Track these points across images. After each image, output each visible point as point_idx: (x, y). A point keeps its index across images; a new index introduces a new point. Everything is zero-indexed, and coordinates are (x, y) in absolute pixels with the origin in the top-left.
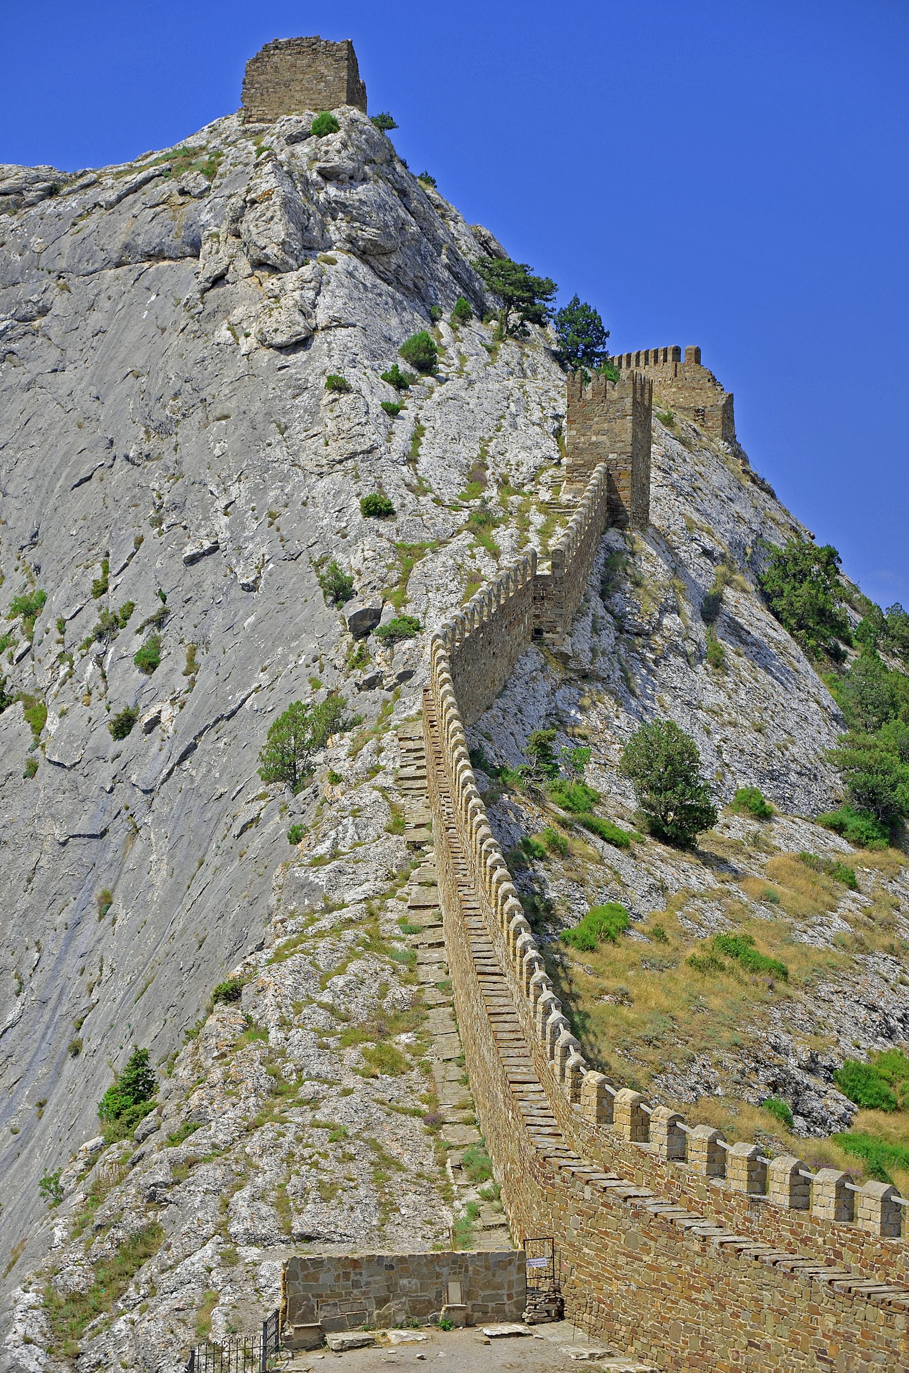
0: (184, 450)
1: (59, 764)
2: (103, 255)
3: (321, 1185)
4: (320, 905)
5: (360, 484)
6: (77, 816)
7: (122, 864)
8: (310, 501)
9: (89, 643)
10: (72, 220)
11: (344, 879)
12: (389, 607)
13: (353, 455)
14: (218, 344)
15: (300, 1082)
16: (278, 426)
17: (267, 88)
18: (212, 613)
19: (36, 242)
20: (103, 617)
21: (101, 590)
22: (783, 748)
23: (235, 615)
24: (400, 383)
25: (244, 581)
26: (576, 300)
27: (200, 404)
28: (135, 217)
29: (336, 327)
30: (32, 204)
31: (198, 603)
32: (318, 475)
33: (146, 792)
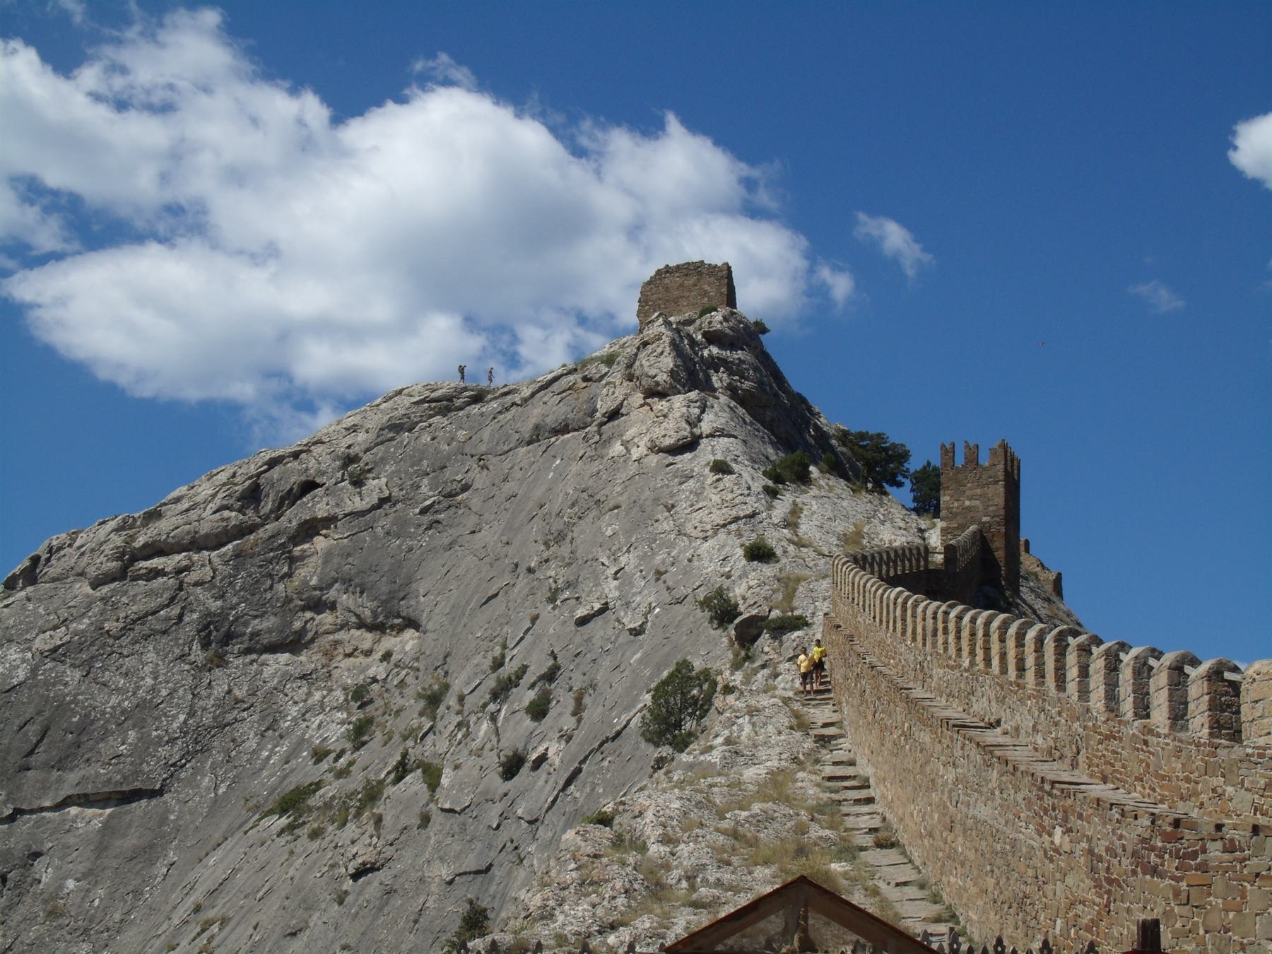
1: (451, 811)
2: (517, 436)
5: (743, 539)
6: (464, 855)
7: (504, 895)
8: (695, 558)
9: (485, 705)
10: (492, 416)
13: (737, 519)
14: (612, 458)
16: (666, 506)
17: (659, 305)
18: (600, 661)
19: (462, 435)
21: (498, 664)
23: (623, 655)
24: (778, 479)
25: (632, 626)
26: (929, 464)
27: (594, 506)
28: (545, 403)
29: (719, 436)
30: (461, 409)
31: (587, 656)
32: (703, 539)
33: (530, 822)
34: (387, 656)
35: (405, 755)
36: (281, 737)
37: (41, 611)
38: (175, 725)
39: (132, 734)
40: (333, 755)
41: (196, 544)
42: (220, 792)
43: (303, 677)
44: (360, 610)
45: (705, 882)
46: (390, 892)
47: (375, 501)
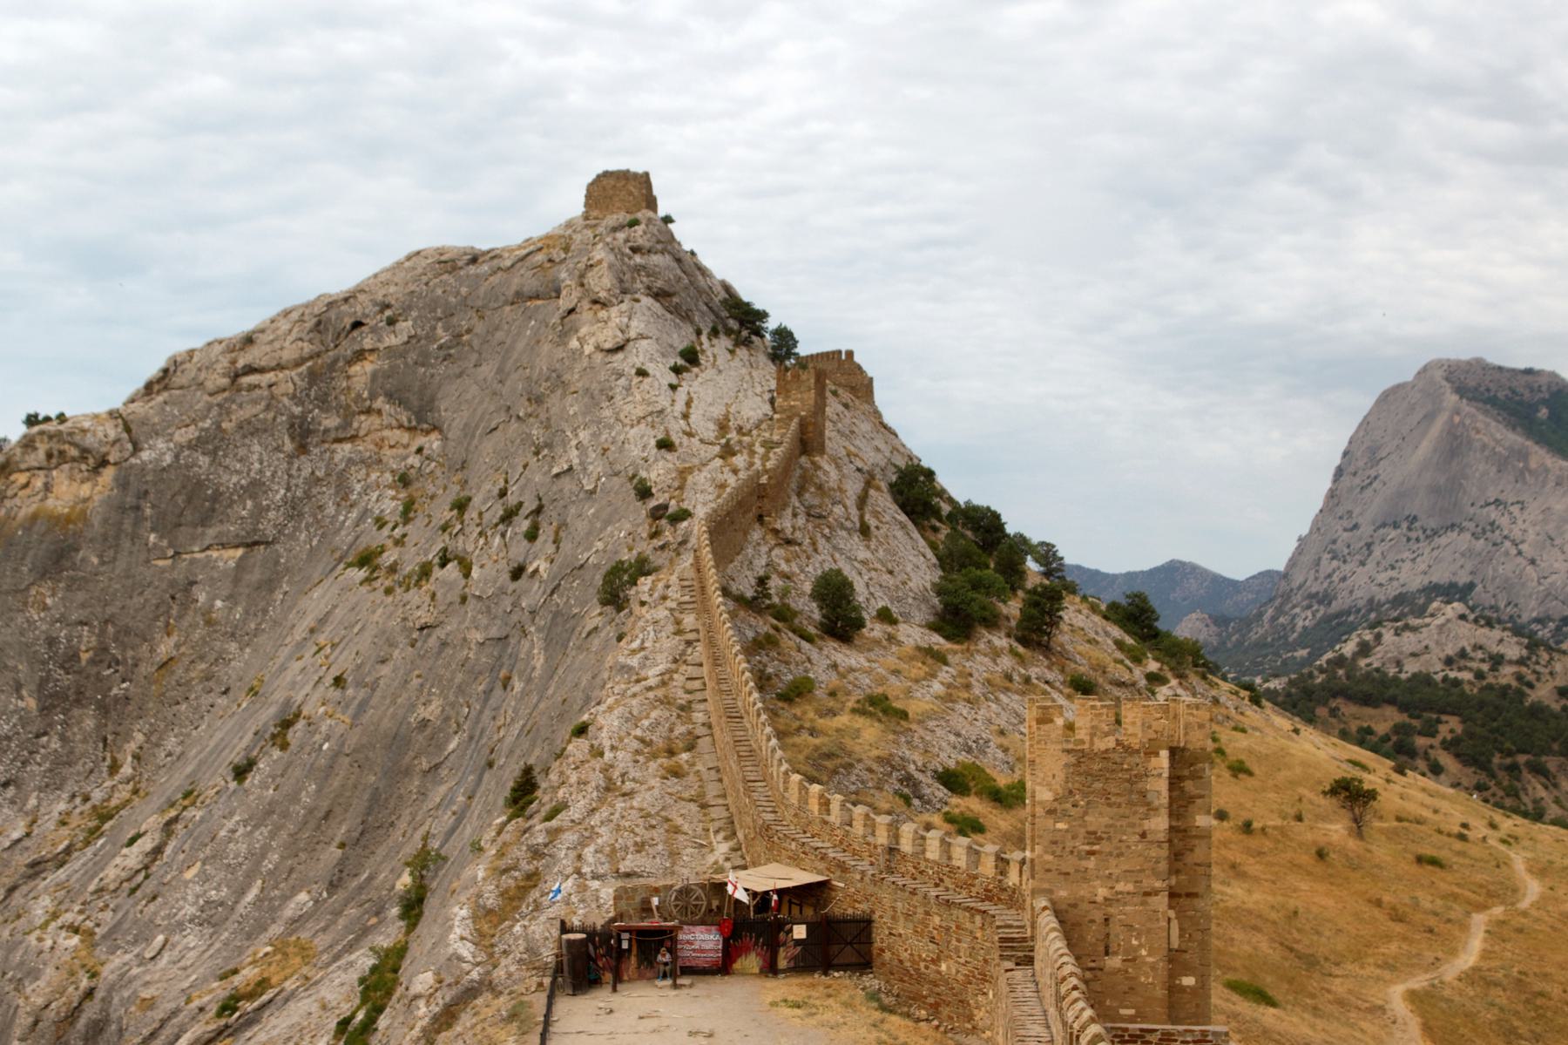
0: (552, 411)
3: (636, 844)
4: (634, 678)
9: (497, 525)
11: (648, 663)
12: (673, 502)
13: (651, 413)
15: (623, 782)
19: (464, 290)
20: (505, 510)
21: (503, 493)
22: (904, 583)
30: (461, 268)
34: (420, 451)
35: (445, 550)
36: (351, 506)
37: (176, 412)
38: (278, 497)
39: (249, 504)
40: (390, 525)
41: (280, 367)
42: (315, 543)
43: (363, 462)
44: (399, 417)
45: (629, 780)
46: (444, 644)
47: (406, 339)
